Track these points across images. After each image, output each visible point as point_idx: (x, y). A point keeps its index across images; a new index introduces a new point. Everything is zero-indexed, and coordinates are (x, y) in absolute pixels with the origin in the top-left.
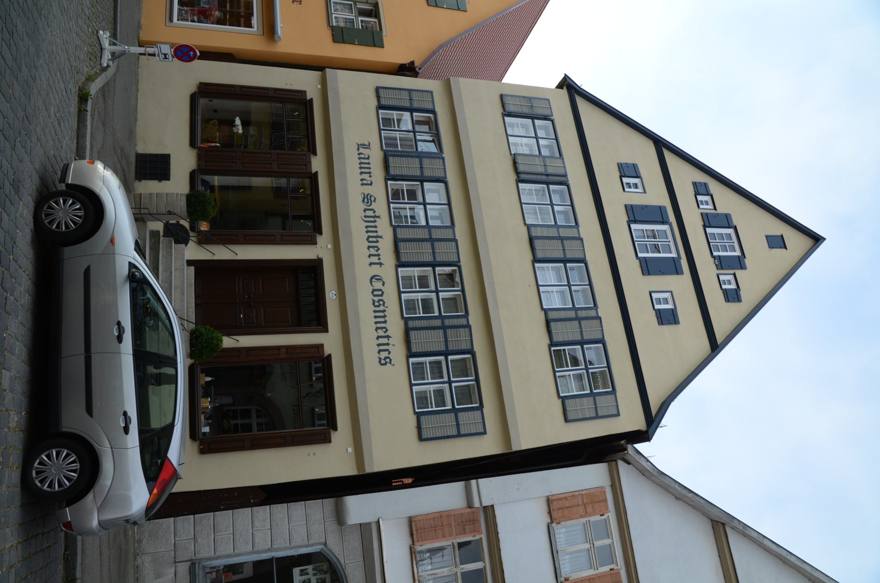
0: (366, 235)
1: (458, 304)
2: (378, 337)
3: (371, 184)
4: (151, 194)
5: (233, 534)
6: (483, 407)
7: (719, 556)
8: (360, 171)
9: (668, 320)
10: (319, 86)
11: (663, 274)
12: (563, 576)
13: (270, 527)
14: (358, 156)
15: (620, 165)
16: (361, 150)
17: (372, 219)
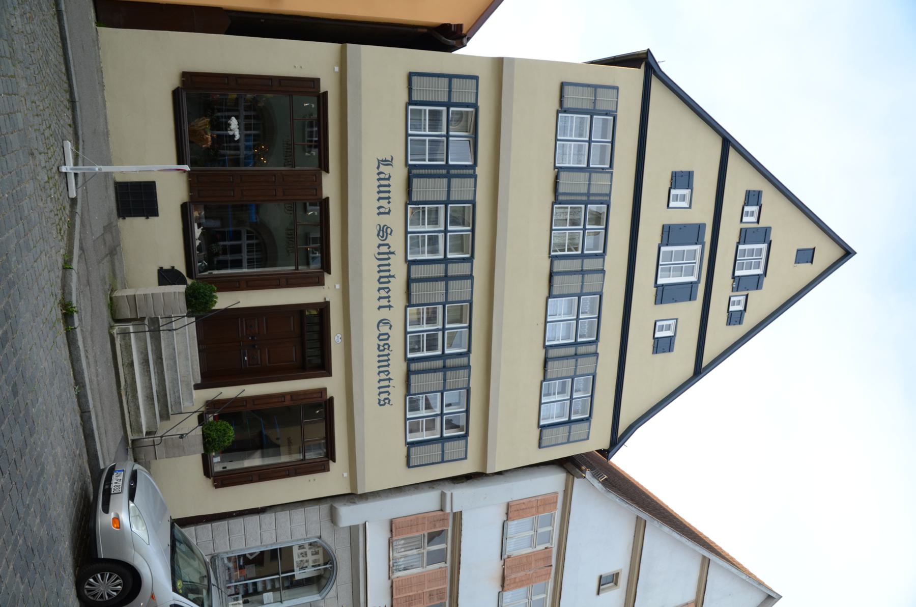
0: (378, 276)
1: (466, 244)
2: (380, 381)
3: (388, 213)
4: (146, 295)
5: (245, 535)
6: (474, 258)
7: (634, 536)
8: (377, 196)
9: (664, 349)
10: (337, 69)
11: (676, 301)
12: (507, 553)
13: (274, 528)
14: (378, 211)
15: (674, 175)
16: (382, 168)
17: (386, 256)
